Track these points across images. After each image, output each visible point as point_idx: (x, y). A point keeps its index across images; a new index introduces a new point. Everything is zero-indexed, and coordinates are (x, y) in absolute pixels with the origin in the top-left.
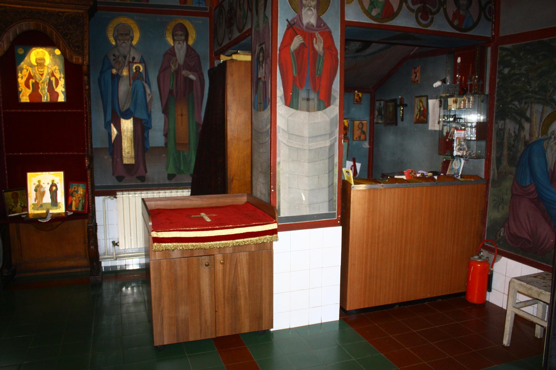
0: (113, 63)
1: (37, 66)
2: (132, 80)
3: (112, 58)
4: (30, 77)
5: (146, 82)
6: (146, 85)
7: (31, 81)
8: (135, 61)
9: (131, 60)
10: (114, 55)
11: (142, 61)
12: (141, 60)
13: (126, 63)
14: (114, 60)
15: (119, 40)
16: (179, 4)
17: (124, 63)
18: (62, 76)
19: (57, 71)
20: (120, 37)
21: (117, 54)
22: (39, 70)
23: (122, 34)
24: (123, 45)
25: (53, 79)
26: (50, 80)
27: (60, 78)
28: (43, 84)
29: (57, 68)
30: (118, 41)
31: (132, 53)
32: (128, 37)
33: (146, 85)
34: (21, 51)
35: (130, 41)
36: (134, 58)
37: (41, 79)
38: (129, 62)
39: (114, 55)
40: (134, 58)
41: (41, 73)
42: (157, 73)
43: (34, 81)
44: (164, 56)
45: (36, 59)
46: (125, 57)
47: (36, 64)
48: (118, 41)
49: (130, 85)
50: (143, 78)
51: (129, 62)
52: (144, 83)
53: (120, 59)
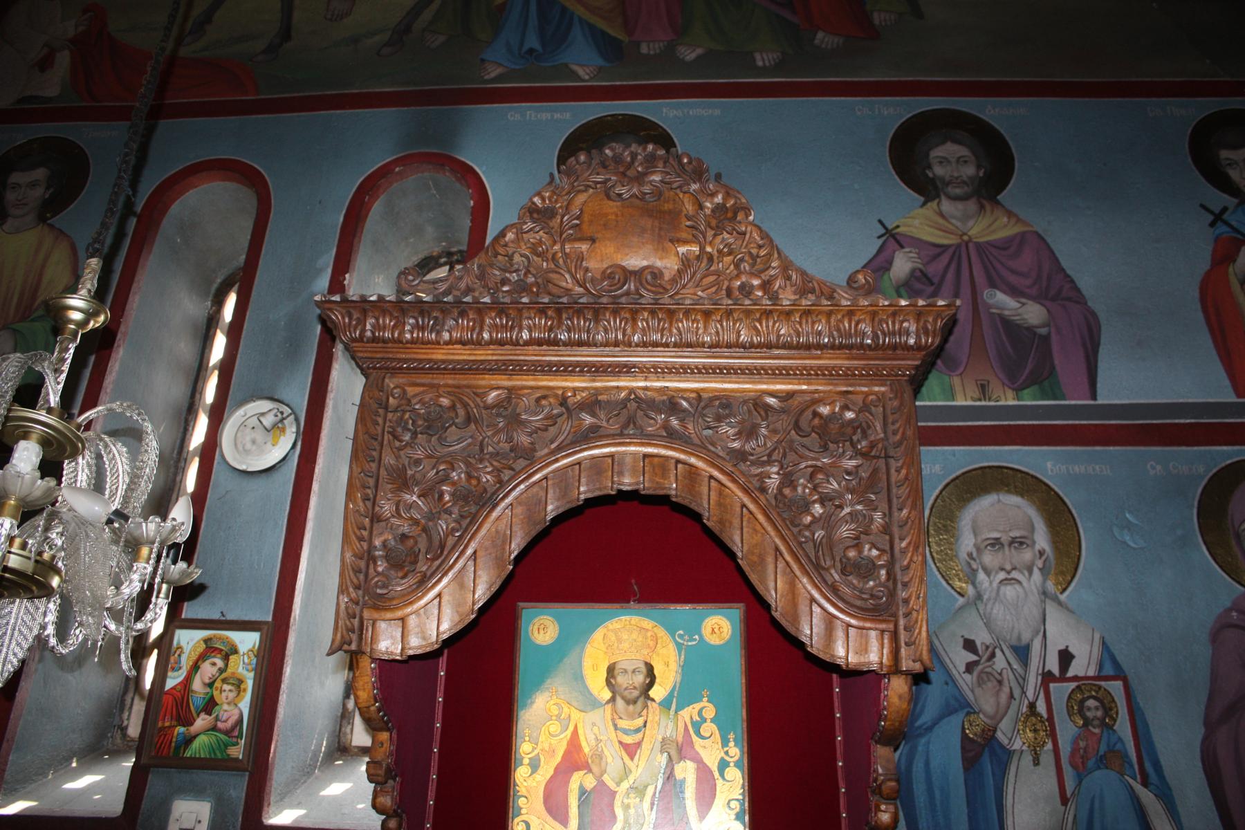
0: (966, 681)
1: (613, 699)
2: (1068, 771)
3: (959, 658)
4: (573, 760)
5: (1145, 783)
6: (1146, 796)
7: (577, 780)
8: (1075, 669)
9: (1053, 665)
10: (969, 645)
11: (1109, 670)
12: (1101, 666)
13: (1033, 680)
14: (970, 667)
15: (988, 572)
16: (1233, 398)
17: (1022, 681)
18: (735, 752)
19: (709, 728)
20: (988, 558)
21: (982, 637)
22: (623, 724)
23: (996, 543)
24: (1009, 591)
25: (686, 771)
26: (670, 776)
27: (723, 765)
28: (633, 800)
29: (710, 712)
30: (981, 576)
31: (1051, 628)
32: (1027, 555)
33: (1146, 796)
34: (541, 627)
35: (1037, 575)
36: (1066, 657)
37: (626, 772)
38: (1047, 677)
39: (969, 645)
40: (1066, 657)
41: (628, 740)
42: (1200, 731)
43: (590, 782)
44: (1215, 636)
45: (611, 670)
46: (1023, 653)
47: (607, 695)
48: (981, 576)
49: (1064, 800)
50: (1124, 756)
51: (1047, 677)
52: (1138, 787)
53: (1000, 662)
